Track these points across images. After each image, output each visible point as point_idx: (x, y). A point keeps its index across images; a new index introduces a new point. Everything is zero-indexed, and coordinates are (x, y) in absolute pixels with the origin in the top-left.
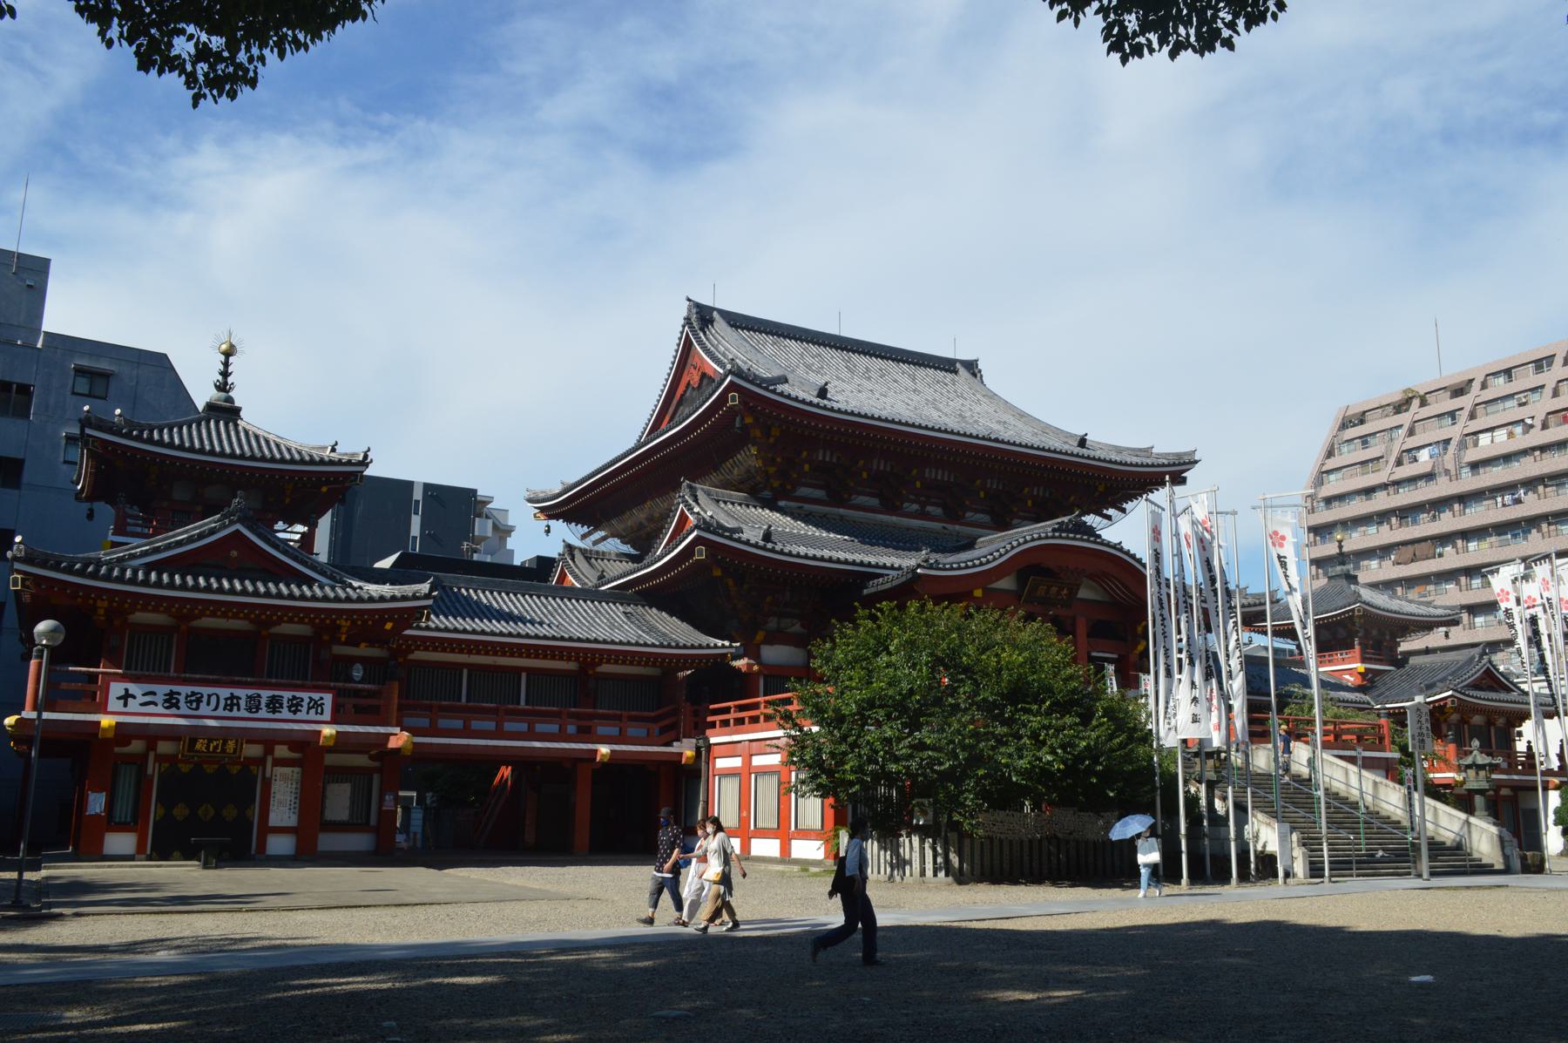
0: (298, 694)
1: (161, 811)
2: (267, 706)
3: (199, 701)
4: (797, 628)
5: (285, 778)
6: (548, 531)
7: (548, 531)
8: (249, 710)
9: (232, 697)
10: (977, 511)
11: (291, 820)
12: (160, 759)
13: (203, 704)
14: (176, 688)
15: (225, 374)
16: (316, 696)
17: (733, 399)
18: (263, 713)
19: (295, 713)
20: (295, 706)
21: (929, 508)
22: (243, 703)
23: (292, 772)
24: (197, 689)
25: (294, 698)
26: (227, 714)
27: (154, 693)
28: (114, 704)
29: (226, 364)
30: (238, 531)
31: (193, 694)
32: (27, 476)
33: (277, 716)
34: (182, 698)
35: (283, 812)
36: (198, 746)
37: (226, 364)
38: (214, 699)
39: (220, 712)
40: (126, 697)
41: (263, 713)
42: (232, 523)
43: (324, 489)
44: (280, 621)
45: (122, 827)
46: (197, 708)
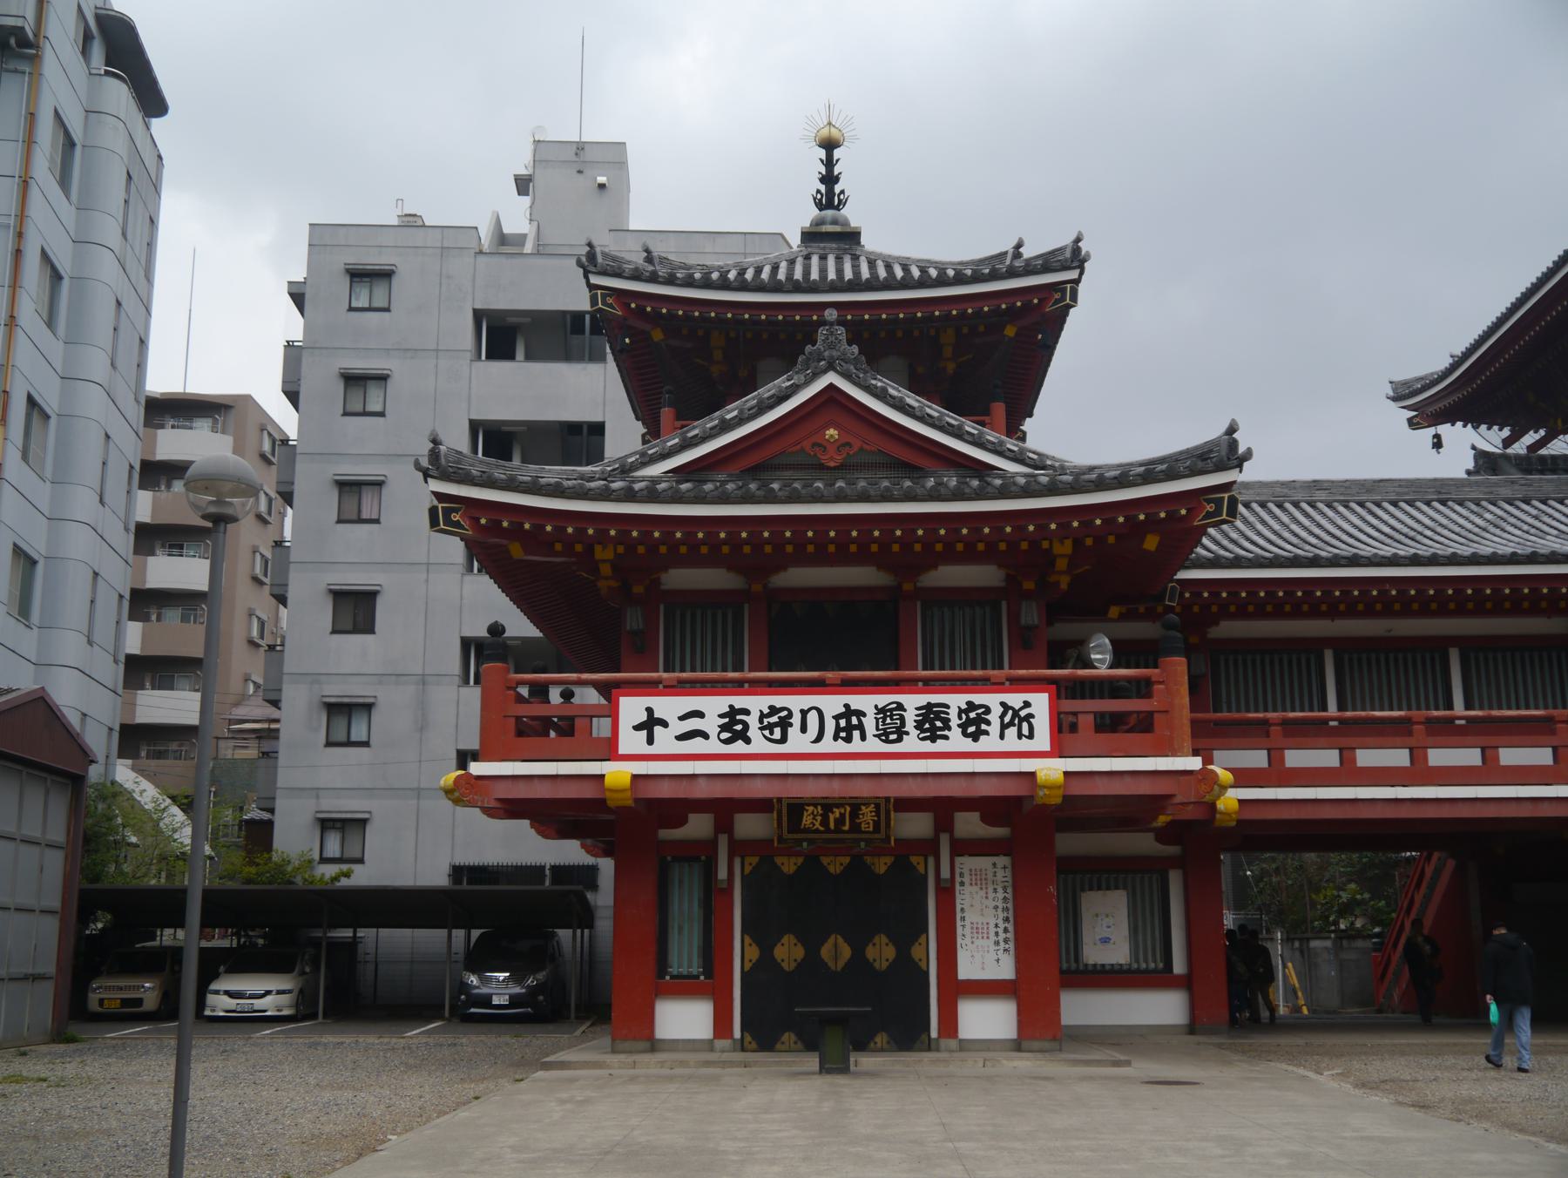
0: (978, 699)
1: (754, 953)
2: (919, 726)
3: (785, 724)
5: (981, 880)
6: (1438, 443)
7: (1438, 443)
8: (884, 736)
9: (849, 712)
11: (1004, 969)
12: (739, 848)
13: (794, 732)
14: (739, 701)
15: (829, 179)
16: (1016, 700)
18: (912, 742)
20: (974, 723)
23: (998, 868)
24: (779, 701)
25: (971, 706)
26: (841, 747)
28: (631, 741)
29: (829, 163)
30: (831, 387)
31: (774, 710)
32: (156, 123)
33: (941, 746)
34: (753, 721)
35: (984, 953)
36: (807, 820)
37: (829, 163)
38: (813, 718)
39: (828, 745)
40: (650, 724)
41: (912, 742)
42: (816, 375)
43: (1010, 331)
45: (685, 988)
46: (783, 740)
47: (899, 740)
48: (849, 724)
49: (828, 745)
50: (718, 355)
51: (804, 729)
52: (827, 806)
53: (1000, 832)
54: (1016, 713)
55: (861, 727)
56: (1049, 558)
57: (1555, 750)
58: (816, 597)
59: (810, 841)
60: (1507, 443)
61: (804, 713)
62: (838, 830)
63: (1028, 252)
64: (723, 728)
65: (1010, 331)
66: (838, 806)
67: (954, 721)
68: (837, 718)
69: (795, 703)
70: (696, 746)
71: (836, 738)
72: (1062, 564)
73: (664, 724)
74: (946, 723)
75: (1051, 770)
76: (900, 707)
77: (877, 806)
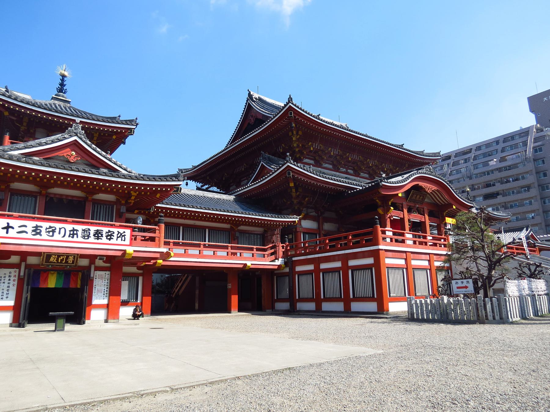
0: (111, 229)
2: (94, 235)
3: (53, 231)
4: (314, 214)
5: (101, 277)
7: (187, 184)
8: (84, 237)
9: (74, 230)
10: (365, 173)
14: (39, 223)
15: (62, 85)
16: (121, 231)
17: (291, 114)
19: (110, 239)
20: (110, 236)
21: (349, 171)
22: (80, 233)
24: (52, 225)
26: (70, 239)
27: (26, 226)
29: (63, 80)
30: (76, 140)
31: (50, 227)
33: (100, 241)
34: (43, 230)
37: (63, 80)
38: (63, 231)
39: (67, 238)
42: (71, 136)
44: (100, 191)
46: (53, 236)
47: (88, 238)
48: (74, 233)
49: (67, 238)
50: (25, 124)
51: (59, 233)
52: (59, 255)
53: (108, 265)
54: (121, 234)
55: (77, 234)
56: (130, 196)
57: (228, 253)
58: (61, 197)
59: (52, 265)
60: (202, 186)
61: (60, 229)
62: (61, 262)
63: (121, 119)
64: (33, 231)
65: (114, 137)
66: (62, 256)
67: (104, 235)
68: (70, 231)
69: (58, 226)
70: (23, 235)
71: (69, 236)
72: (133, 198)
73: (13, 228)
74: (102, 235)
75: (130, 250)
76: (89, 230)
77: (74, 256)
